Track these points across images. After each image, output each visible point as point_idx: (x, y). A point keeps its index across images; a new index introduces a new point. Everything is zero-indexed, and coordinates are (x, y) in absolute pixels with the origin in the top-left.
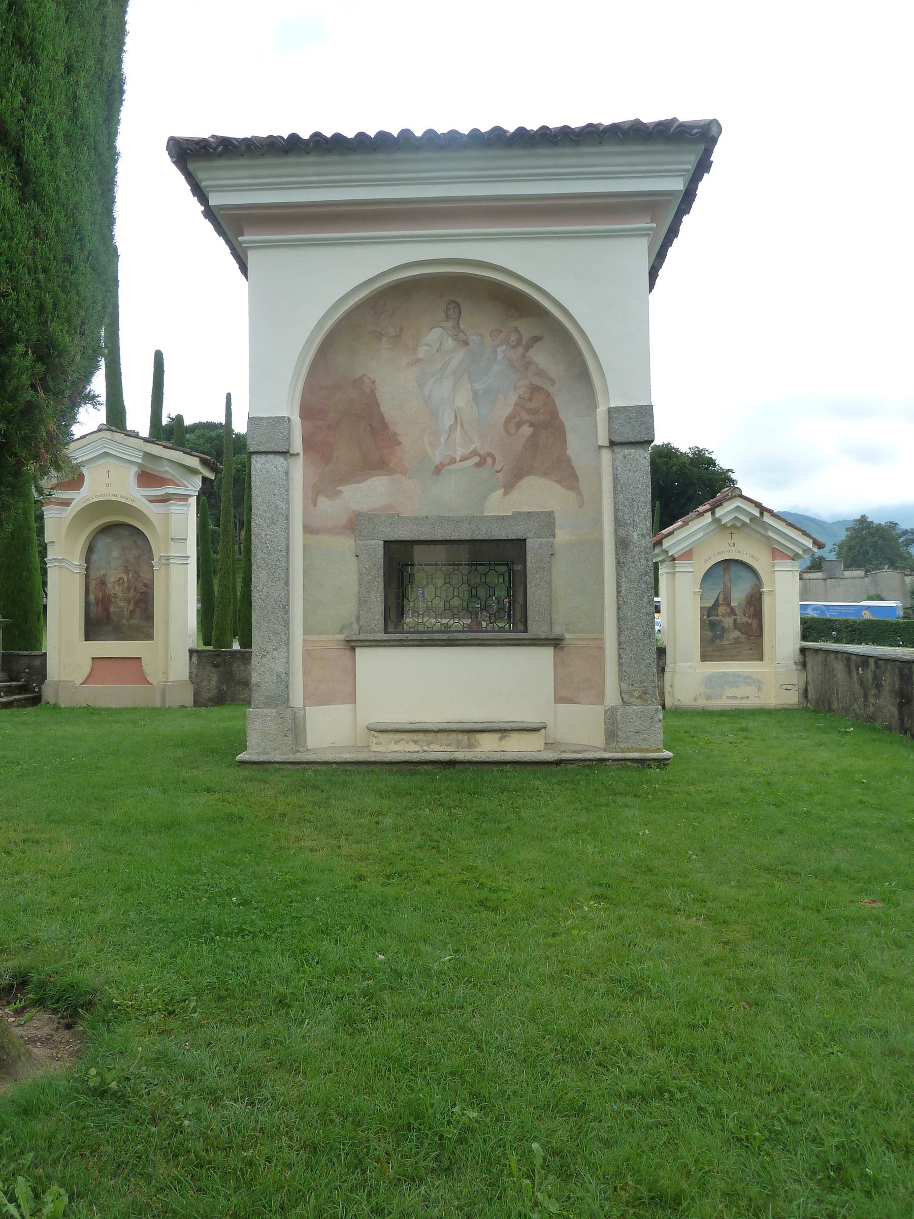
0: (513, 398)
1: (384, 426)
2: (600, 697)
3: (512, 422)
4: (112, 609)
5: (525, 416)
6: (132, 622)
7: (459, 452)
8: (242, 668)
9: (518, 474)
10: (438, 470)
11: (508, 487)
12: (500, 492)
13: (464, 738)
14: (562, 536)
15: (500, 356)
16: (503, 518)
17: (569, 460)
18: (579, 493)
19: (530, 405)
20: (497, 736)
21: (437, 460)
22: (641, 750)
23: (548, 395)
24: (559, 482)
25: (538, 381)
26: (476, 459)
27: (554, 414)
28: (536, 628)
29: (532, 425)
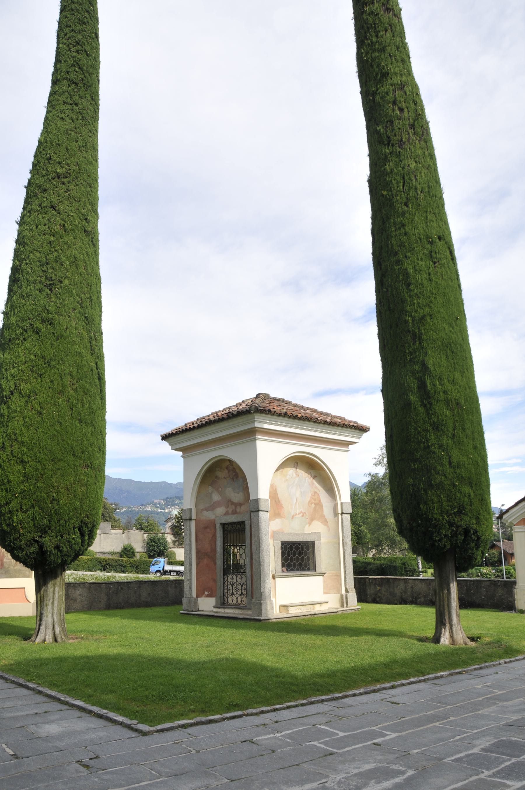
0: (310, 495)
1: (279, 502)
2: (339, 590)
3: (310, 503)
4: (5, 560)
5: (313, 501)
6: (16, 568)
7: (298, 512)
8: (74, 591)
9: (312, 519)
10: (293, 517)
11: (310, 524)
12: (308, 525)
13: (312, 606)
14: (323, 540)
15: (307, 481)
16: (309, 534)
17: (324, 516)
18: (328, 527)
19: (314, 498)
20: (319, 605)
21: (292, 514)
22: (353, 606)
23: (318, 495)
24: (322, 523)
25: (316, 490)
26: (302, 514)
27: (320, 501)
28: (318, 570)
29: (314, 504)
